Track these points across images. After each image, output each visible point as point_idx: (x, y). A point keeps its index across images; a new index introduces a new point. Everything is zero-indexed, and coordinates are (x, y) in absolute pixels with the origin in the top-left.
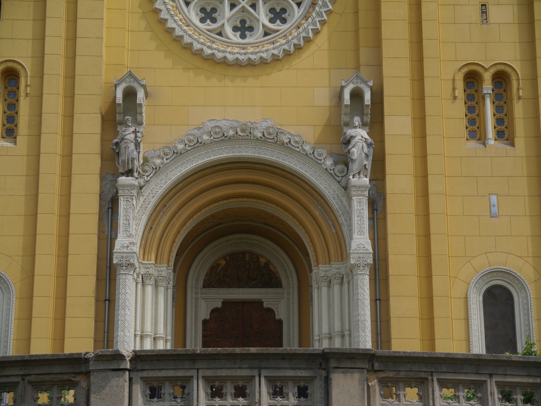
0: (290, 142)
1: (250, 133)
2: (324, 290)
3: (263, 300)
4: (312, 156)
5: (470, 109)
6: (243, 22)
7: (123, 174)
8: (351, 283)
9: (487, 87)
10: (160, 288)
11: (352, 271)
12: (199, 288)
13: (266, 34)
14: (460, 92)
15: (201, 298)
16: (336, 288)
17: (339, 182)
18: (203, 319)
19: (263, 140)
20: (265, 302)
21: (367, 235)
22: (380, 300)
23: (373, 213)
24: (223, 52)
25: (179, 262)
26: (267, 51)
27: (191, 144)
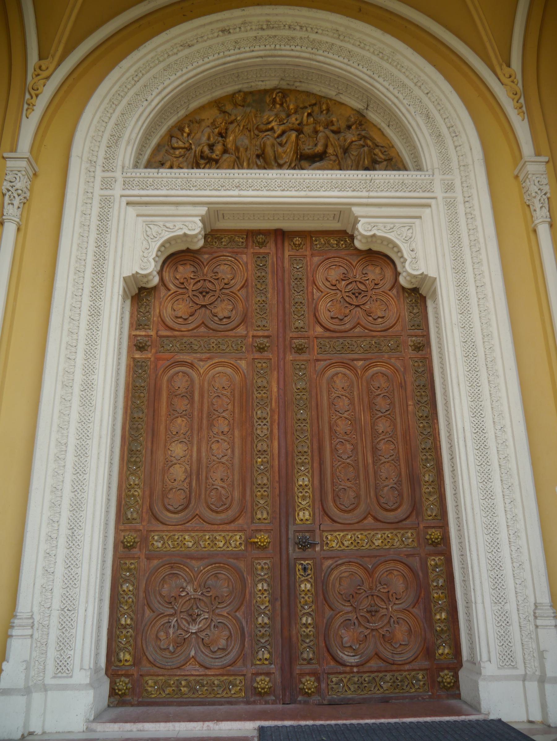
3: (356, 211)
12: (119, 168)
15: (124, 200)
18: (127, 273)
20: (362, 221)
25: (48, 78)
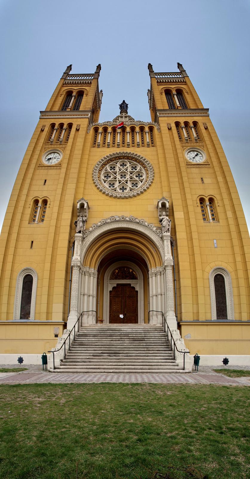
0: (140, 222)
1: (125, 219)
2: (154, 278)
4: (148, 227)
5: (203, 211)
6: (123, 187)
7: (77, 233)
8: (165, 274)
9: (207, 203)
10: (91, 277)
11: (165, 269)
13: (131, 190)
14: (199, 204)
16: (159, 276)
17: (159, 236)
19: (130, 221)
21: (170, 254)
22: (176, 280)
23: (172, 247)
24: (116, 194)
26: (131, 194)
27: (104, 223)
